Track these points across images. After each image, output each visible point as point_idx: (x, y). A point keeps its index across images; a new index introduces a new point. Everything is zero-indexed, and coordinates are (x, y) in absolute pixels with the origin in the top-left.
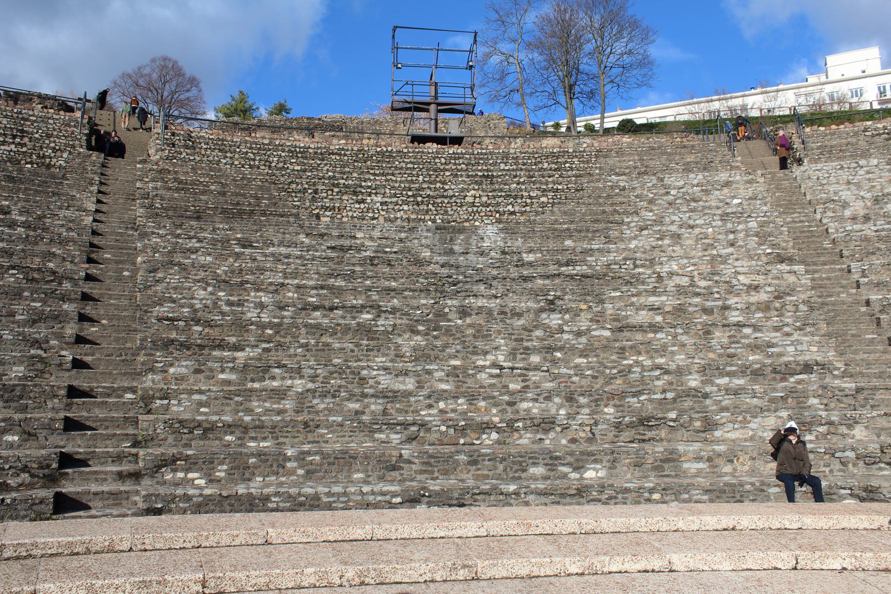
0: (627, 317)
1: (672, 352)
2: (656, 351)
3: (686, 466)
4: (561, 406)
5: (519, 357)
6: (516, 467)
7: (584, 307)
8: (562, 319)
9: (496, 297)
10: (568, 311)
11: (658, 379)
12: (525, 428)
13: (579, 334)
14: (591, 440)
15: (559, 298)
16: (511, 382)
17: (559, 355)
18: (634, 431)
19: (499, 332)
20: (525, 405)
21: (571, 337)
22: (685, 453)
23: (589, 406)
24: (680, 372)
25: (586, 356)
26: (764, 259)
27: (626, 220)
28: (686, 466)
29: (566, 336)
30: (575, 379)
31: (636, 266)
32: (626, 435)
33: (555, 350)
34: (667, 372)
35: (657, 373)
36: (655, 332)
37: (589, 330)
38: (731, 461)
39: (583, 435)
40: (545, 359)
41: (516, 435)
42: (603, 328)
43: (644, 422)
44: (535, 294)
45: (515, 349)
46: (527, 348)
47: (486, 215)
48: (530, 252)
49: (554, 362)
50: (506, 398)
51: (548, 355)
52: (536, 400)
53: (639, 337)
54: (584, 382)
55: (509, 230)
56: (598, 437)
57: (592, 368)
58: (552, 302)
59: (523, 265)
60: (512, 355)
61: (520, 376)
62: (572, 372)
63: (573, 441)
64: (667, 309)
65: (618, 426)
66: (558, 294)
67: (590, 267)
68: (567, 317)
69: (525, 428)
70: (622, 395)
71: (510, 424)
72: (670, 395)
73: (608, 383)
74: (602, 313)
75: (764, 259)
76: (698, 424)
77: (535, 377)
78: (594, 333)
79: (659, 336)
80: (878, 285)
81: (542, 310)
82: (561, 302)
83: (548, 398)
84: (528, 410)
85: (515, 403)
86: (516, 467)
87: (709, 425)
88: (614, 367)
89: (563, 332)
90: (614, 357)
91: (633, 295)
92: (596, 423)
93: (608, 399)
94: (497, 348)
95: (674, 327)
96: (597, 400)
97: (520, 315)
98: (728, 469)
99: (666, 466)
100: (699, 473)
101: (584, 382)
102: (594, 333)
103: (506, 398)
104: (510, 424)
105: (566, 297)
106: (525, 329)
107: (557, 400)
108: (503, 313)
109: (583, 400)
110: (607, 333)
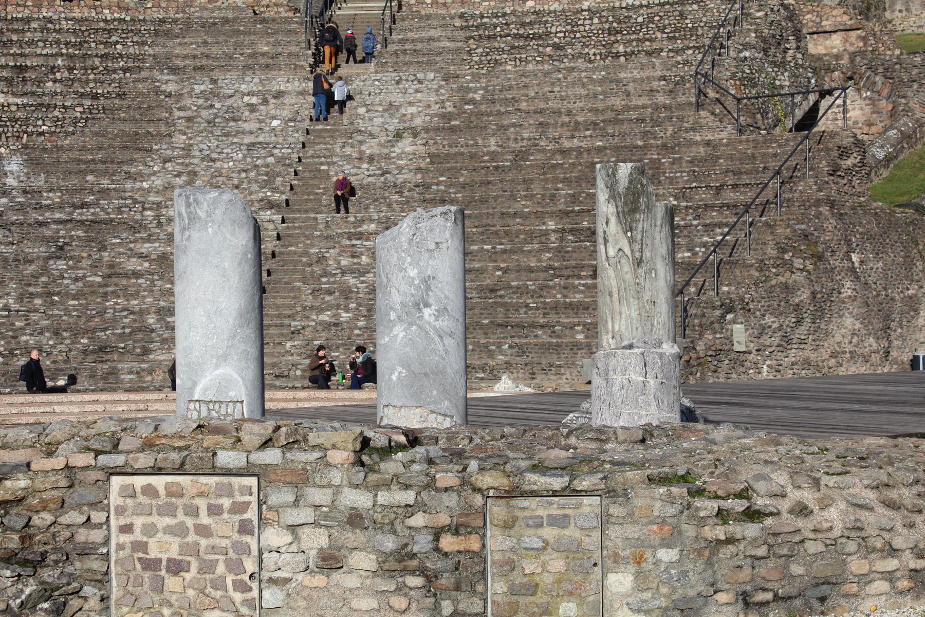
0: (120, 263)
1: (144, 297)
2: (131, 295)
3: (122, 377)
4: (50, 339)
5: (25, 300)
6: (12, 379)
7: (85, 255)
8: (67, 264)
9: (13, 244)
10: (71, 258)
11: (126, 317)
12: (21, 354)
13: (76, 280)
14: (67, 361)
15: (65, 244)
16: (17, 321)
17: (56, 298)
18: (96, 355)
19: (12, 279)
20: (24, 338)
21: (70, 282)
22: (122, 369)
23: (69, 338)
24: (142, 312)
25: (77, 299)
26: (257, 205)
27: (155, 147)
28: (122, 377)
29: (66, 282)
30: (64, 318)
31: (144, 209)
32: (91, 358)
33: (53, 294)
34: (132, 313)
35: (125, 313)
36: (137, 278)
37: (84, 277)
38: (151, 374)
39: (61, 358)
40: (45, 301)
41: (15, 359)
42: (96, 275)
43: (103, 349)
44: (46, 240)
45: (22, 295)
46: (32, 294)
47: (13, 136)
48: (50, 191)
49: (53, 303)
50: (11, 333)
51: (48, 299)
52: (32, 335)
53: (124, 282)
54: (71, 320)
55: (34, 163)
56: (71, 359)
57: (77, 310)
58: (61, 248)
59: (41, 208)
60: (20, 299)
61: (23, 316)
62: (62, 313)
63: (54, 362)
64: (153, 257)
65: (85, 352)
66: (67, 240)
67: (103, 209)
68: (71, 263)
69: (21, 354)
70: (94, 331)
71: (11, 352)
72: (127, 331)
73: (88, 321)
74: (101, 259)
75: (257, 205)
76: (138, 350)
77: (34, 317)
78: (88, 279)
79: (140, 281)
80: (327, 238)
81: (50, 258)
82: (69, 248)
83: (41, 333)
84: (27, 342)
85: (17, 337)
86: (12, 379)
87: (146, 351)
88: (94, 310)
89: (63, 278)
90: (99, 300)
91: (131, 242)
92: (70, 350)
93: (84, 333)
94: (8, 294)
95: (152, 274)
96: (75, 334)
97: (31, 262)
98: (149, 378)
99: (110, 377)
100: (131, 381)
101: (71, 320)
102: (88, 279)
103: (11, 333)
104: (11, 352)
105: (74, 244)
106: (33, 276)
107: (47, 334)
108: (16, 260)
109: (65, 334)
110: (99, 279)
